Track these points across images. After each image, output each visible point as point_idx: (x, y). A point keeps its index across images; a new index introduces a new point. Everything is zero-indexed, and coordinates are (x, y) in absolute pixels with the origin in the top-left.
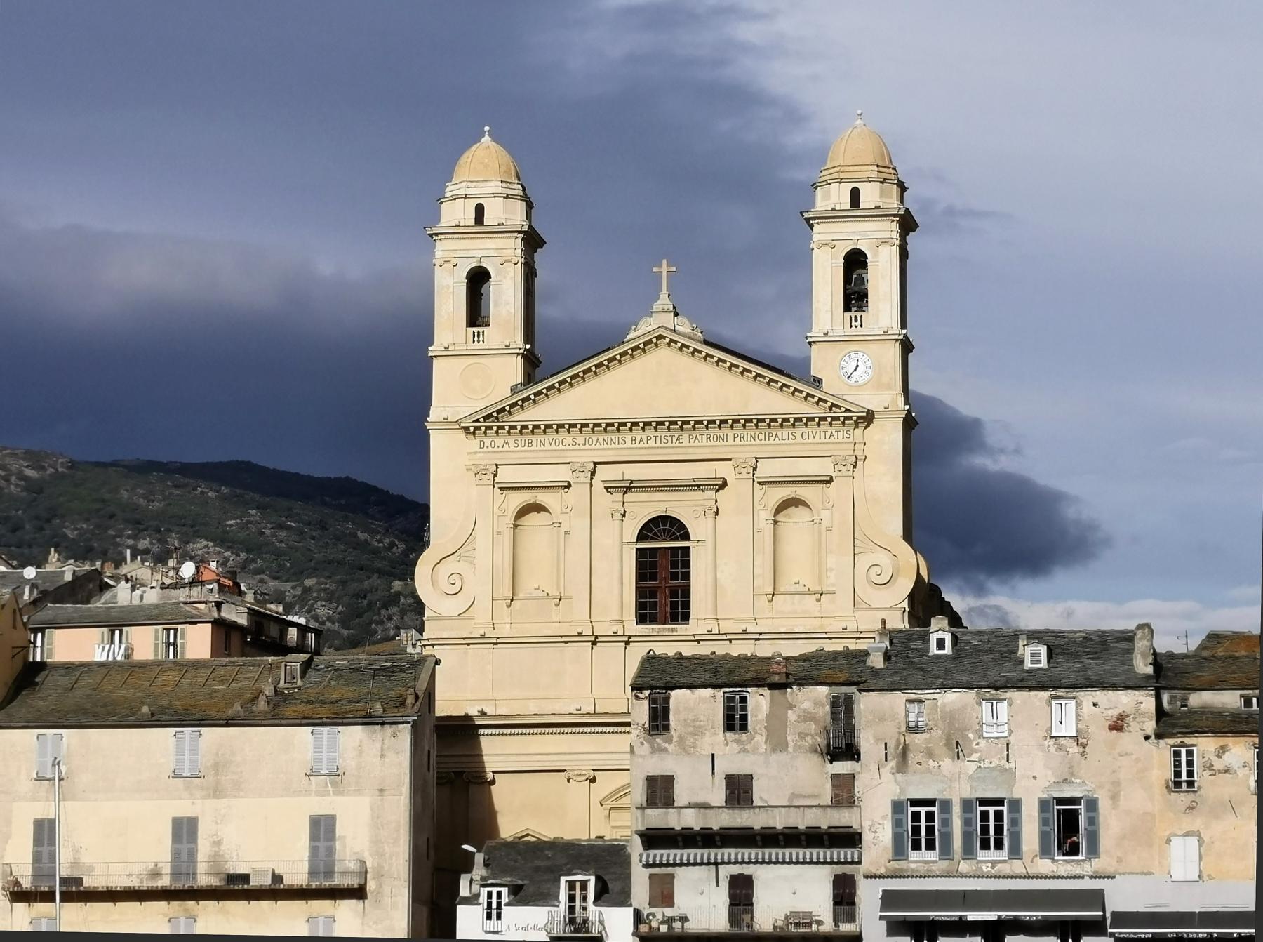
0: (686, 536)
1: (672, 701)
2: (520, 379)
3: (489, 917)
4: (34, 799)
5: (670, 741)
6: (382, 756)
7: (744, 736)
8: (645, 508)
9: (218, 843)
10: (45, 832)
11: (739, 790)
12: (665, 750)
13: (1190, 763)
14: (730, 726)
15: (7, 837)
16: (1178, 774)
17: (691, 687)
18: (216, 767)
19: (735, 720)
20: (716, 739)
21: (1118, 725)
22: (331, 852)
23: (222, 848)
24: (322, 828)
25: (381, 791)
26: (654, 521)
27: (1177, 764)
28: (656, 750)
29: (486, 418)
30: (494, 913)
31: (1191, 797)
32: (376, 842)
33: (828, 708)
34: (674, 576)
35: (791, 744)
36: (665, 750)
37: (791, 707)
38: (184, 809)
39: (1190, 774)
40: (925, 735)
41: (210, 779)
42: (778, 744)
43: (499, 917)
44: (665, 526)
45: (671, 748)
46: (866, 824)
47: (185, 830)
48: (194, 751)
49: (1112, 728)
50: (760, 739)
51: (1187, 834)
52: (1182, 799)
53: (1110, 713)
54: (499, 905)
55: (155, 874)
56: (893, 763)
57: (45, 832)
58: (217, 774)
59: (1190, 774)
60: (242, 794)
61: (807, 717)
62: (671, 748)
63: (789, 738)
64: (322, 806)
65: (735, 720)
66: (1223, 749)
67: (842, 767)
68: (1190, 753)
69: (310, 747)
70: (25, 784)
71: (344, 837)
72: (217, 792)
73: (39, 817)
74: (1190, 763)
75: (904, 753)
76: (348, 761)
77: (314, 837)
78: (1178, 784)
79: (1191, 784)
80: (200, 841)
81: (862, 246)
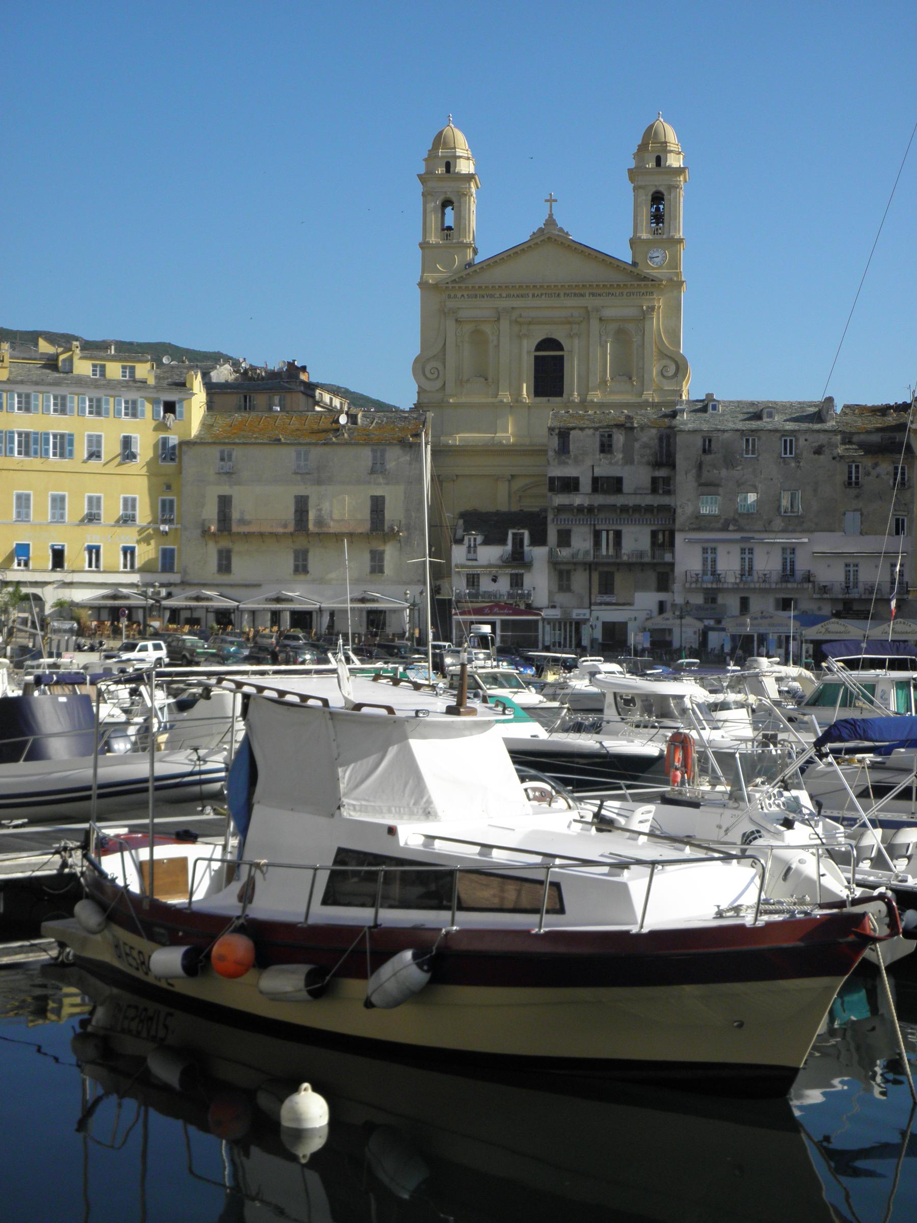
1: (571, 436)
3: (469, 552)
5: (569, 458)
8: (540, 334)
9: (320, 510)
10: (225, 502)
13: (857, 472)
14: (603, 450)
16: (850, 478)
17: (582, 429)
19: (606, 447)
21: (818, 451)
23: (323, 512)
24: (377, 506)
27: (850, 473)
29: (454, 281)
30: (472, 550)
31: (858, 491)
33: (656, 441)
35: (636, 461)
37: (637, 440)
38: (301, 490)
39: (857, 478)
40: (713, 456)
42: (628, 460)
43: (475, 552)
44: (550, 343)
46: (678, 504)
49: (815, 453)
50: (620, 456)
51: (855, 510)
52: (853, 492)
53: (814, 444)
54: (475, 545)
55: (285, 526)
57: (225, 502)
59: (857, 478)
61: (645, 446)
62: (570, 462)
63: (636, 457)
64: (378, 492)
65: (606, 447)
66: (876, 465)
67: (662, 473)
68: (857, 467)
72: (319, 482)
74: (857, 472)
75: (700, 466)
78: (850, 484)
79: (857, 483)
81: (662, 189)
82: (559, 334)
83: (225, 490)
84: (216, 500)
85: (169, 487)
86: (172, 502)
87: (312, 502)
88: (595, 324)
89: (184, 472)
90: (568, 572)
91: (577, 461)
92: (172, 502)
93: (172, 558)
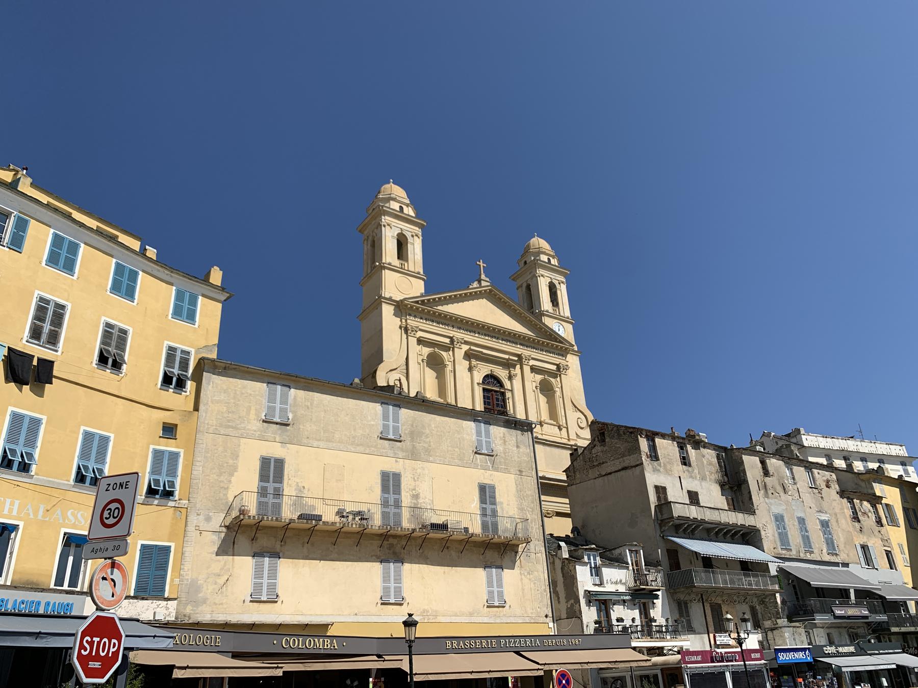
0: (501, 385)
2: (423, 291)
4: (262, 439)
6: (518, 447)
7: (690, 469)
9: (416, 497)
10: (271, 470)
11: (694, 498)
12: (659, 470)
15: (234, 469)
18: (412, 434)
20: (679, 468)
22: (494, 513)
23: (421, 501)
25: (520, 471)
26: (487, 376)
28: (655, 470)
32: (521, 509)
34: (498, 405)
36: (659, 470)
38: (390, 465)
41: (407, 444)
45: (662, 470)
47: (390, 483)
48: (396, 420)
50: (696, 471)
56: (762, 492)
57: (271, 470)
58: (412, 440)
60: (431, 459)
69: (474, 431)
70: (255, 425)
71: (502, 503)
72: (414, 455)
73: (265, 454)
76: (498, 447)
77: (483, 500)
80: (403, 493)
81: (554, 281)
82: (502, 373)
83: (275, 450)
84: (256, 466)
85: (169, 430)
86: (174, 456)
87: (406, 483)
88: (527, 369)
89: (202, 407)
90: (686, 603)
91: (668, 472)
92: (174, 456)
93: (163, 567)
